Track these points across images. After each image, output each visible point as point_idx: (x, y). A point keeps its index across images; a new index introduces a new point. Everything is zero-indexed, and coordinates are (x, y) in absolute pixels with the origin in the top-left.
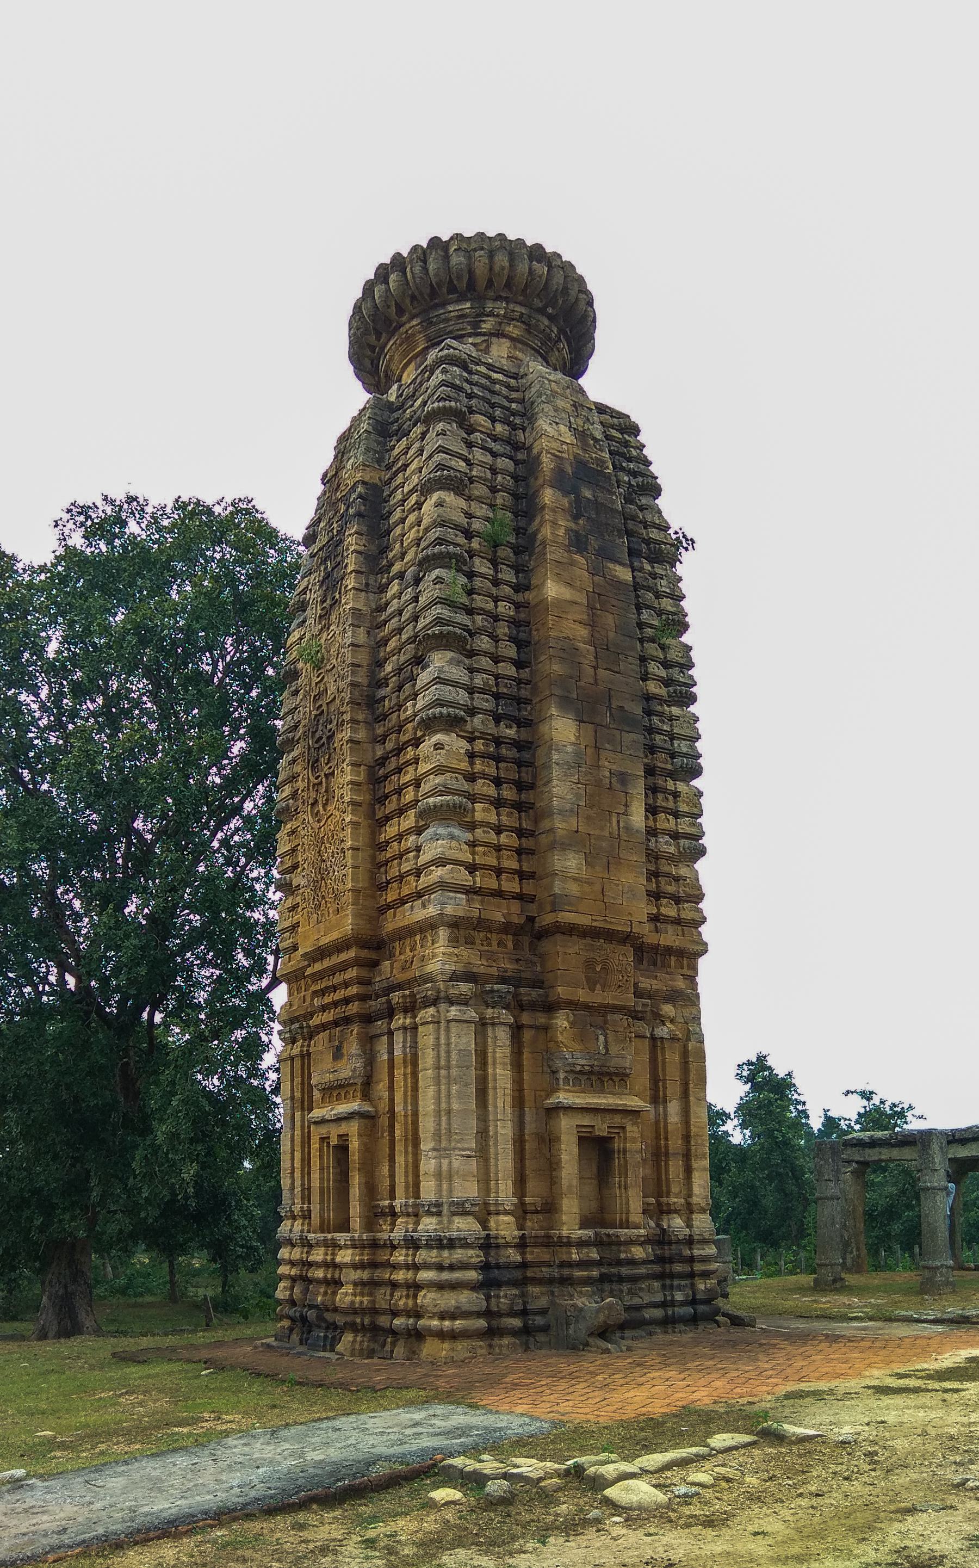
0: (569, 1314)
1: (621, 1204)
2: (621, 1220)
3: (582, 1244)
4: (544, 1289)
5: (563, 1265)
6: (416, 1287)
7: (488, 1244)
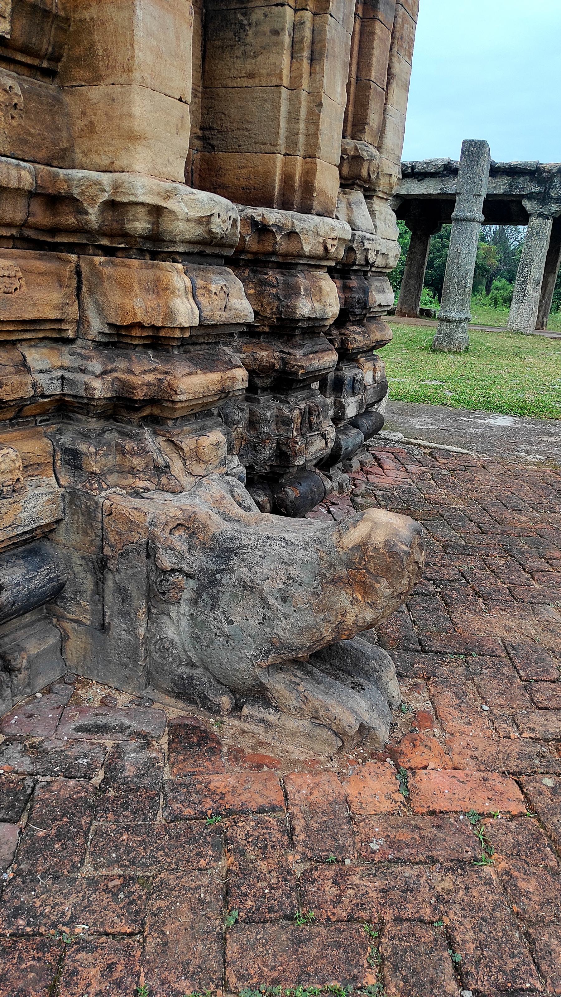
0: (167, 561)
1: (293, 118)
2: (288, 179)
3: (208, 252)
4: (37, 447)
5: (120, 339)
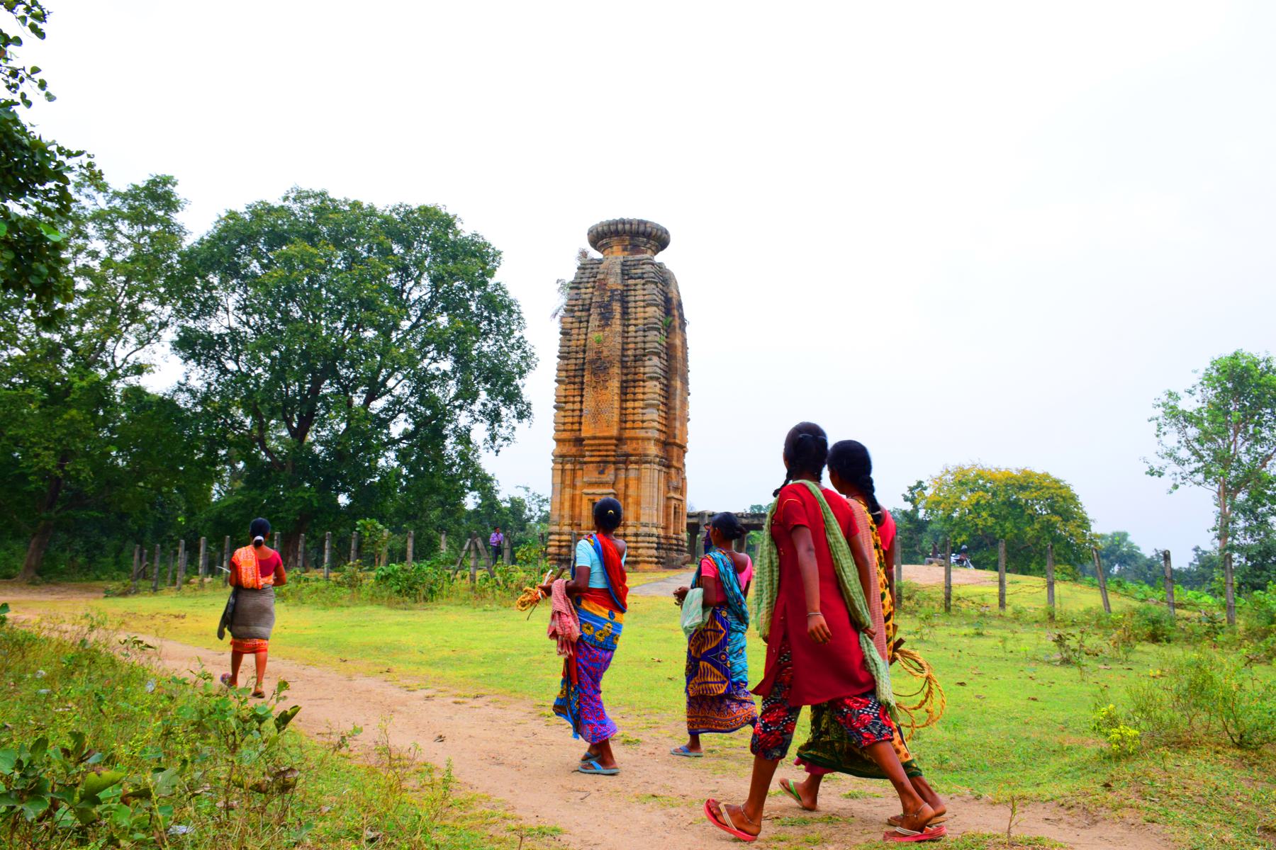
6: (637, 548)
7: (658, 537)
